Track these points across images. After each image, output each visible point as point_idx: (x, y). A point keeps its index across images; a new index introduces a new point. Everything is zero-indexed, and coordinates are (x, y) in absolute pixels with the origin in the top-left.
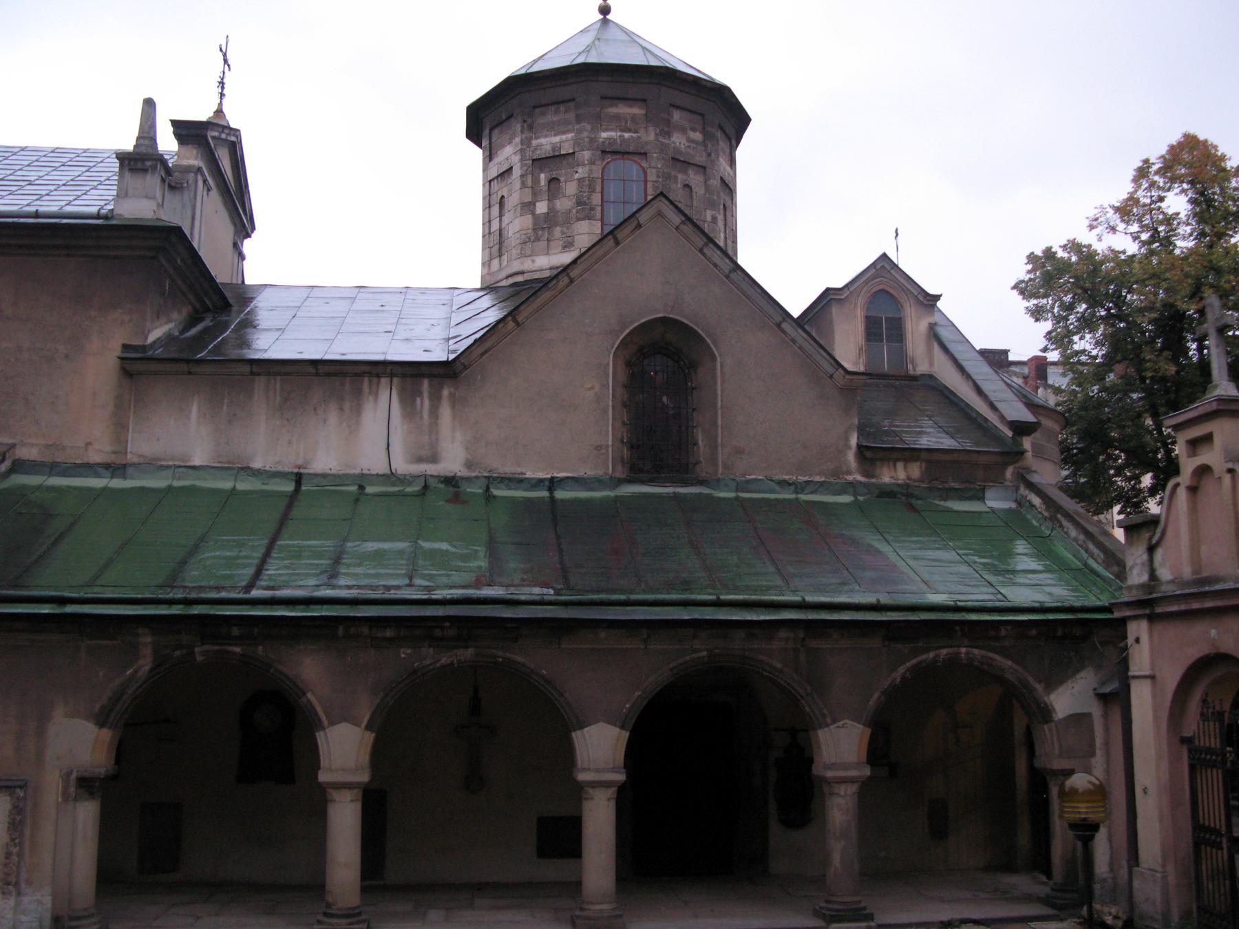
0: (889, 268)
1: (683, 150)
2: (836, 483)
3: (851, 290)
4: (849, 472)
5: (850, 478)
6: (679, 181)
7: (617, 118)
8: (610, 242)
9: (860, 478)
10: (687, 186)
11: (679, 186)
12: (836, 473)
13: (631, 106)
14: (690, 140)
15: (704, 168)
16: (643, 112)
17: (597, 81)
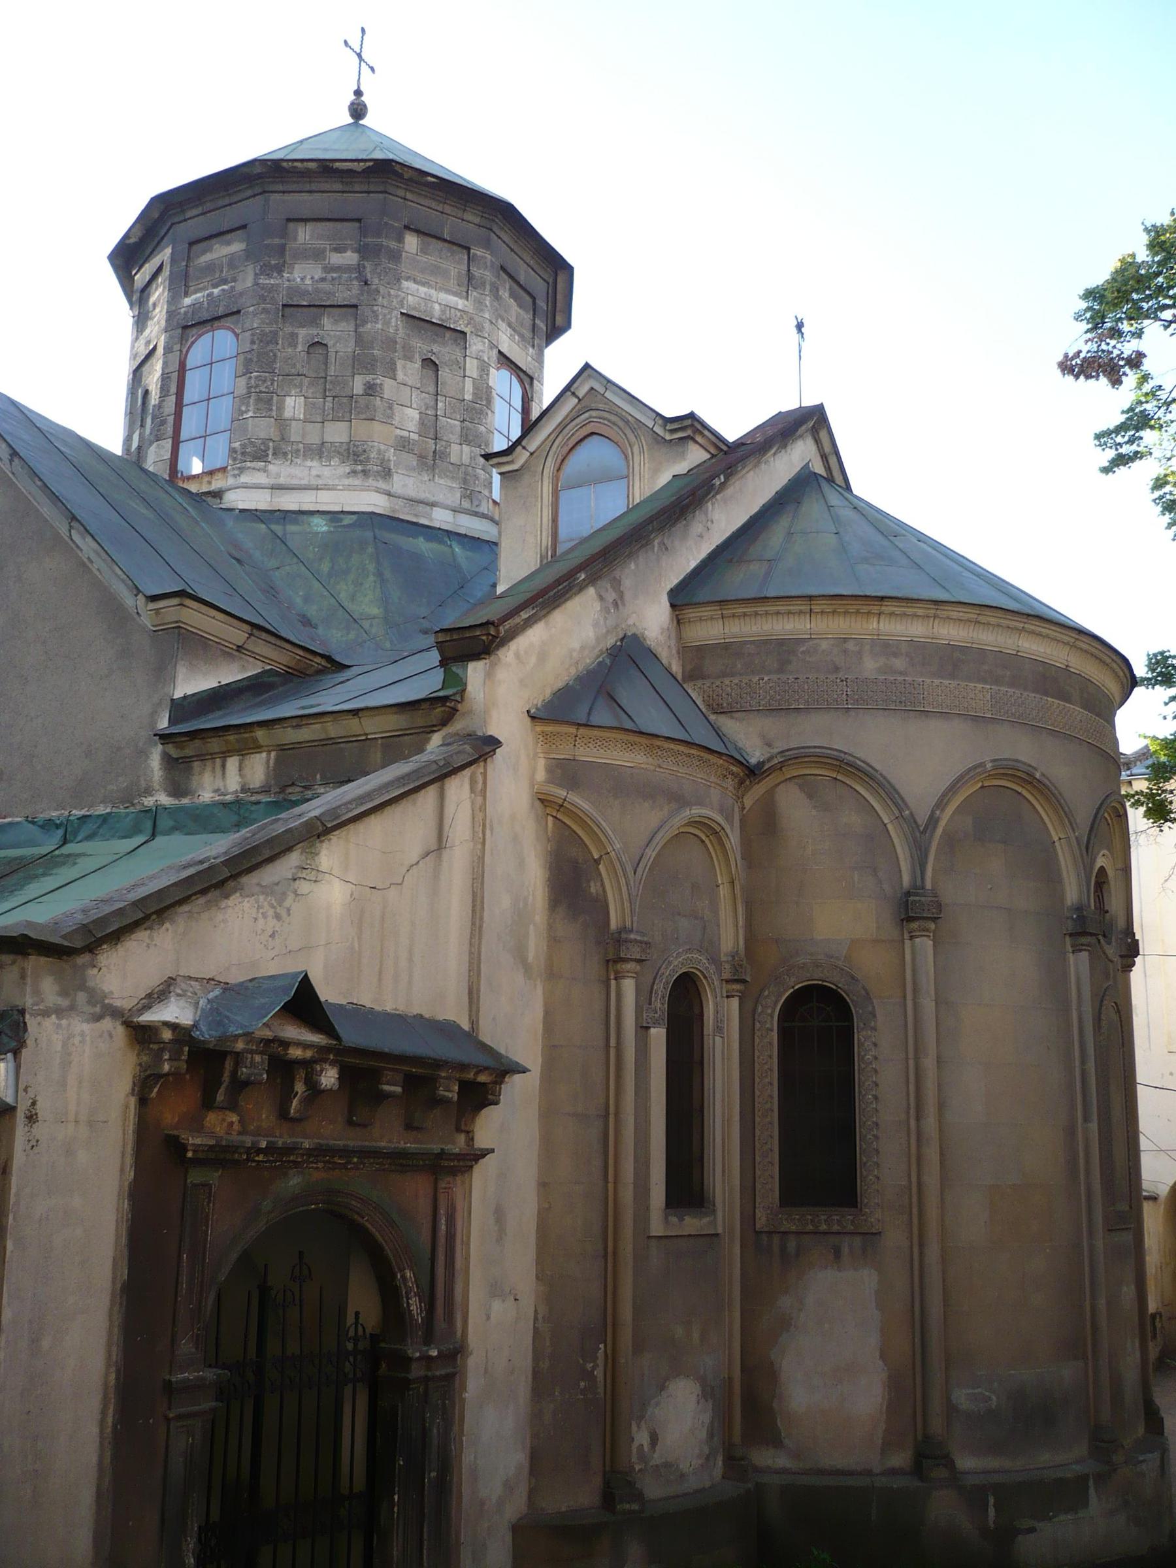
0: (602, 390)
1: (310, 288)
2: (127, 814)
3: (532, 448)
4: (148, 792)
5: (149, 802)
6: (300, 340)
7: (210, 268)
9: (164, 799)
10: (317, 345)
11: (300, 348)
12: (128, 798)
13: (229, 243)
14: (329, 269)
15: (355, 306)
16: (242, 246)
17: (185, 220)
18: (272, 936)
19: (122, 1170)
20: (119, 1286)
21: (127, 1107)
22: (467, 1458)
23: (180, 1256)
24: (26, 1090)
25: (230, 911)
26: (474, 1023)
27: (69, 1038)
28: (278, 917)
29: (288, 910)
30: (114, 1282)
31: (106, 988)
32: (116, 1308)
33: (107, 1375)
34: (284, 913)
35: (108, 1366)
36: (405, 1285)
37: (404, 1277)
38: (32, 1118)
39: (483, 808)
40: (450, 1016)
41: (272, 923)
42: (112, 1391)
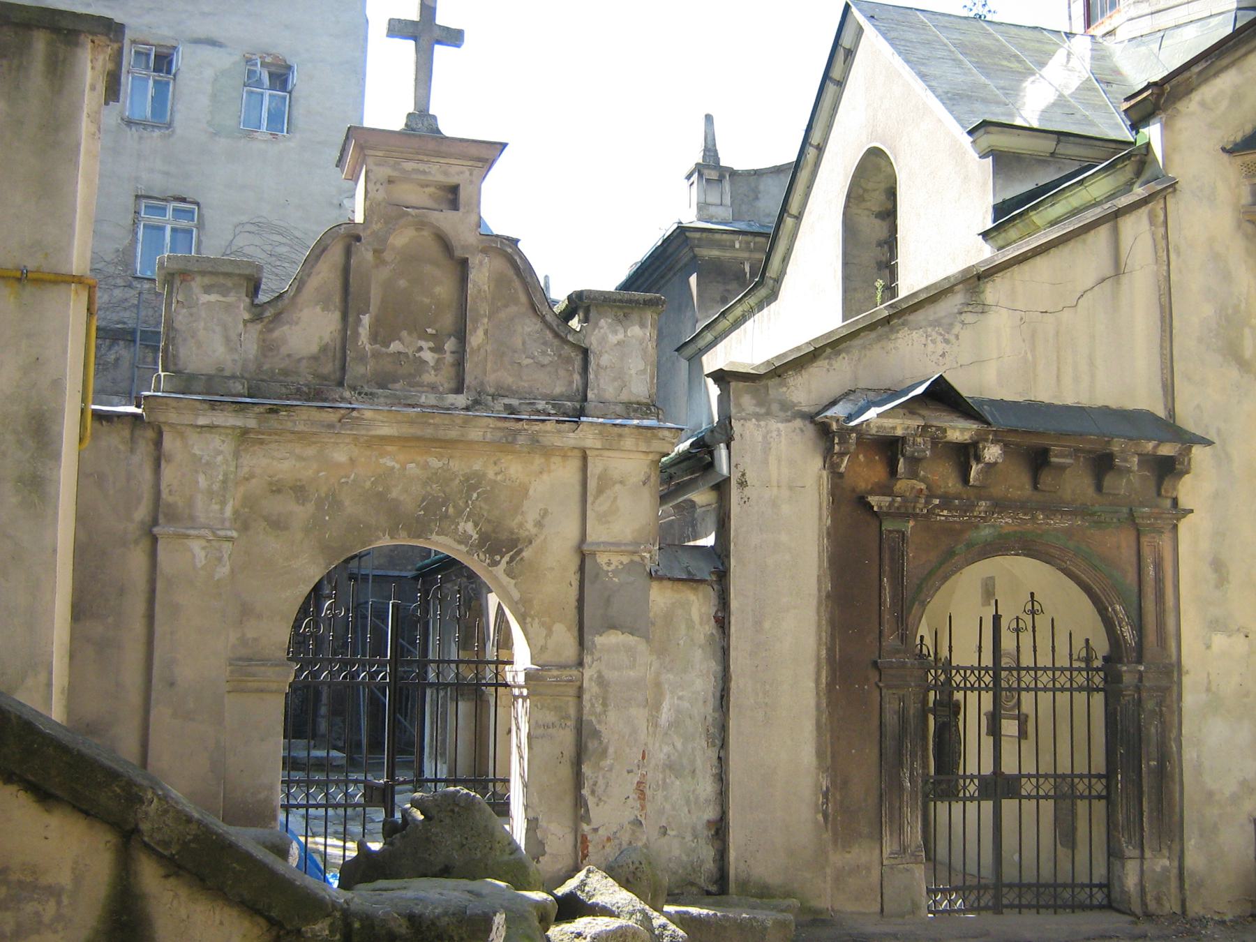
8: (831, 88)
18: (943, 355)
19: (820, 518)
20: (824, 594)
21: (821, 477)
22: (1189, 755)
23: (881, 580)
24: (736, 466)
25: (899, 341)
26: (1171, 412)
27: (768, 433)
28: (947, 341)
29: (957, 337)
30: (819, 590)
31: (795, 400)
32: (823, 609)
33: (819, 651)
34: (952, 338)
35: (819, 645)
36: (1117, 616)
37: (1114, 610)
38: (743, 484)
39: (1166, 237)
40: (1142, 404)
41: (941, 347)
42: (824, 662)
